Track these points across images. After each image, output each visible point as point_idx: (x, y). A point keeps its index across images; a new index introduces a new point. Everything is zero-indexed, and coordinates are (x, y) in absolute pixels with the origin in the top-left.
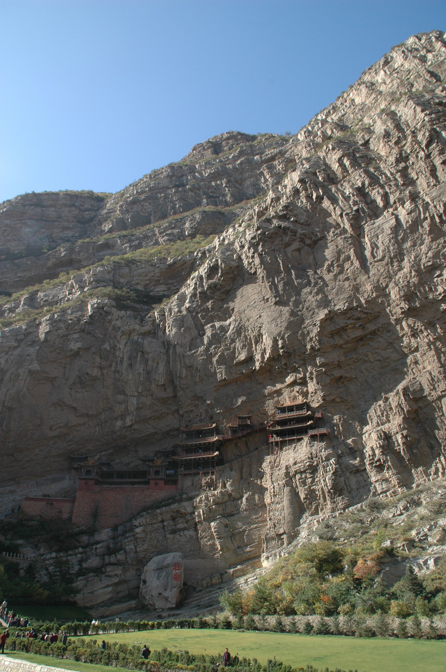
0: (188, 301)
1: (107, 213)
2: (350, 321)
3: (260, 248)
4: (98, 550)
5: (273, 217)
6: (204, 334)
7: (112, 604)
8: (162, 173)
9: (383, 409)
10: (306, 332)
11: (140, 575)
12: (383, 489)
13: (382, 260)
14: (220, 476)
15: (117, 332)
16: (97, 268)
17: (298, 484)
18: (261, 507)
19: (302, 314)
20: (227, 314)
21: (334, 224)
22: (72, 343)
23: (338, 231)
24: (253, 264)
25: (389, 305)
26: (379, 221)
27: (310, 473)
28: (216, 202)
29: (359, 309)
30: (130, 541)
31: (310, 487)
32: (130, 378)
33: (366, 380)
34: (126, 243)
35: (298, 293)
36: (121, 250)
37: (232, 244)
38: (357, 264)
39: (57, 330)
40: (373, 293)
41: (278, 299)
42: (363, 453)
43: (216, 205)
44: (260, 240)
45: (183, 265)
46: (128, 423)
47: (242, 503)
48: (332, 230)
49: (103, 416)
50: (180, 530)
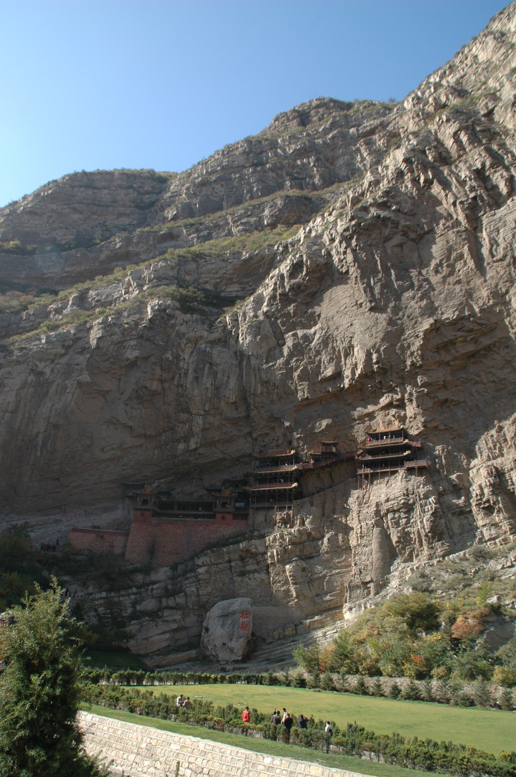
0: (265, 304)
1: (171, 197)
2: (459, 334)
3: (354, 243)
4: (154, 592)
5: (371, 205)
6: (284, 344)
7: (169, 653)
8: (237, 148)
9: (495, 440)
10: (406, 345)
11: (202, 622)
12: (491, 535)
13: (502, 260)
14: (299, 512)
15: (181, 339)
16: (158, 262)
17: (390, 524)
18: (346, 550)
19: (403, 324)
20: (312, 320)
21: (445, 214)
22: (129, 352)
23: (449, 224)
24: (344, 261)
25: (509, 315)
26: (501, 212)
27: (405, 513)
28: (301, 185)
29: (471, 319)
30: (192, 583)
31: (404, 529)
32: (196, 394)
33: (477, 405)
34: (194, 233)
35: (398, 298)
36: (186, 242)
37: (321, 236)
38: (471, 264)
39: (111, 336)
40: (489, 299)
41: (373, 304)
43: (302, 188)
44: (354, 232)
45: (261, 260)
46: (193, 446)
47: (322, 543)
48: (442, 222)
49: (163, 438)
50: (249, 572)
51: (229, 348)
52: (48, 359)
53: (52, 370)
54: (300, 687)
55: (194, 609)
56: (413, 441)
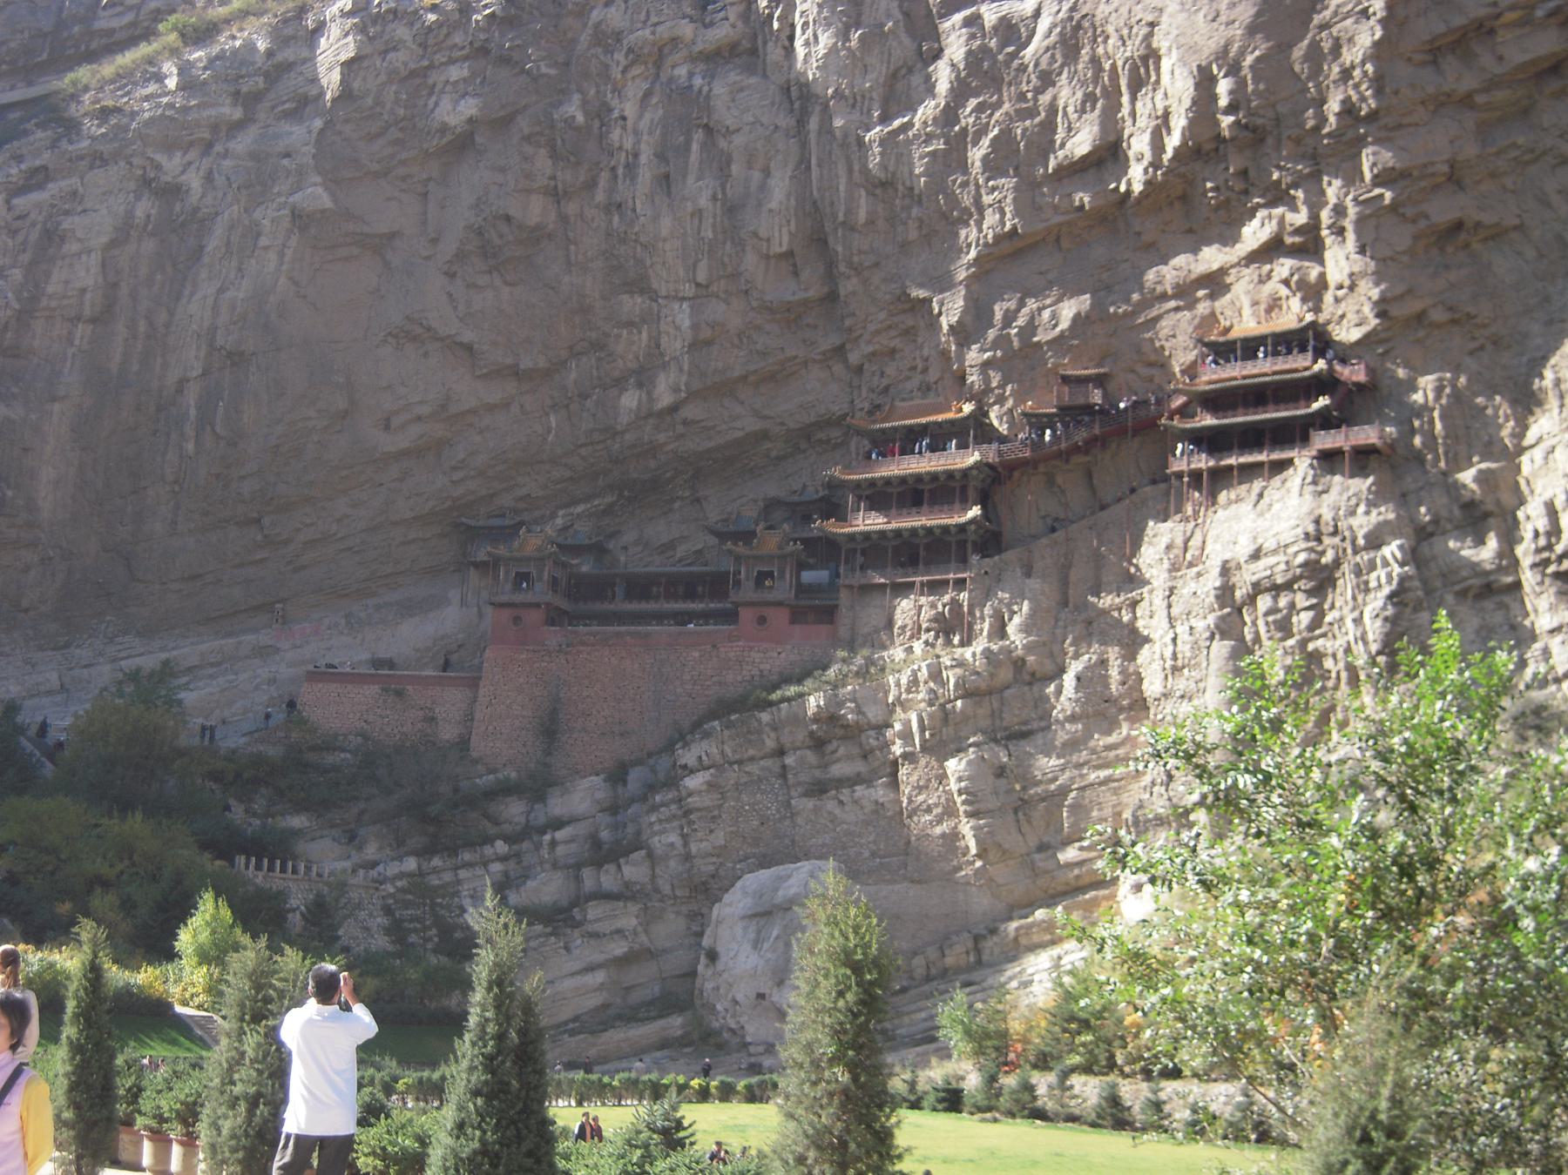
4: (560, 850)
6: (938, 54)
7: (606, 1025)
10: (1326, 46)
11: (701, 934)
14: (988, 594)
15: (609, 51)
18: (1130, 708)
22: (446, 104)
27: (1310, 593)
30: (668, 820)
31: (1303, 644)
32: (665, 232)
39: (386, 52)
42: (1516, 522)
46: (665, 399)
47: (1059, 692)
49: (573, 375)
50: (841, 783)
51: (765, 76)
52: (191, 144)
53: (209, 178)
54: (947, 1110)
55: (675, 897)
56: (1344, 361)
